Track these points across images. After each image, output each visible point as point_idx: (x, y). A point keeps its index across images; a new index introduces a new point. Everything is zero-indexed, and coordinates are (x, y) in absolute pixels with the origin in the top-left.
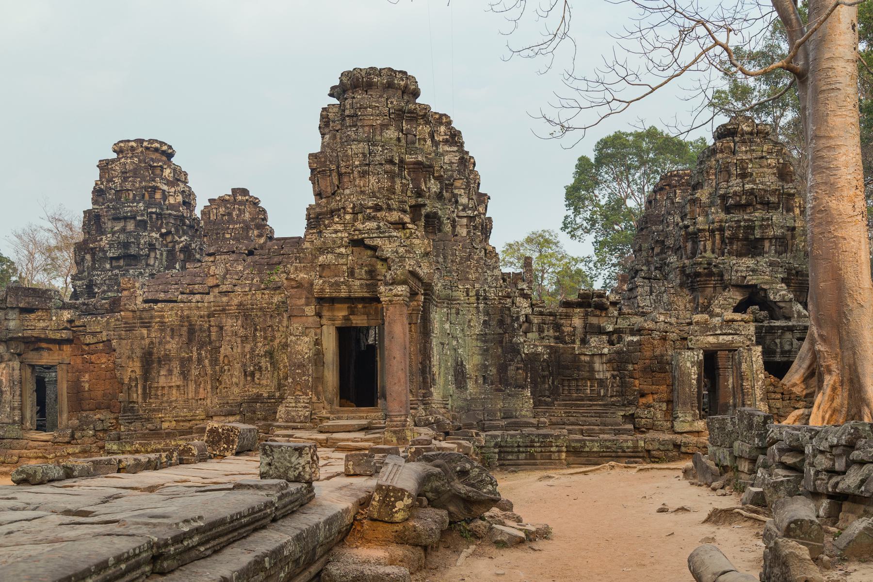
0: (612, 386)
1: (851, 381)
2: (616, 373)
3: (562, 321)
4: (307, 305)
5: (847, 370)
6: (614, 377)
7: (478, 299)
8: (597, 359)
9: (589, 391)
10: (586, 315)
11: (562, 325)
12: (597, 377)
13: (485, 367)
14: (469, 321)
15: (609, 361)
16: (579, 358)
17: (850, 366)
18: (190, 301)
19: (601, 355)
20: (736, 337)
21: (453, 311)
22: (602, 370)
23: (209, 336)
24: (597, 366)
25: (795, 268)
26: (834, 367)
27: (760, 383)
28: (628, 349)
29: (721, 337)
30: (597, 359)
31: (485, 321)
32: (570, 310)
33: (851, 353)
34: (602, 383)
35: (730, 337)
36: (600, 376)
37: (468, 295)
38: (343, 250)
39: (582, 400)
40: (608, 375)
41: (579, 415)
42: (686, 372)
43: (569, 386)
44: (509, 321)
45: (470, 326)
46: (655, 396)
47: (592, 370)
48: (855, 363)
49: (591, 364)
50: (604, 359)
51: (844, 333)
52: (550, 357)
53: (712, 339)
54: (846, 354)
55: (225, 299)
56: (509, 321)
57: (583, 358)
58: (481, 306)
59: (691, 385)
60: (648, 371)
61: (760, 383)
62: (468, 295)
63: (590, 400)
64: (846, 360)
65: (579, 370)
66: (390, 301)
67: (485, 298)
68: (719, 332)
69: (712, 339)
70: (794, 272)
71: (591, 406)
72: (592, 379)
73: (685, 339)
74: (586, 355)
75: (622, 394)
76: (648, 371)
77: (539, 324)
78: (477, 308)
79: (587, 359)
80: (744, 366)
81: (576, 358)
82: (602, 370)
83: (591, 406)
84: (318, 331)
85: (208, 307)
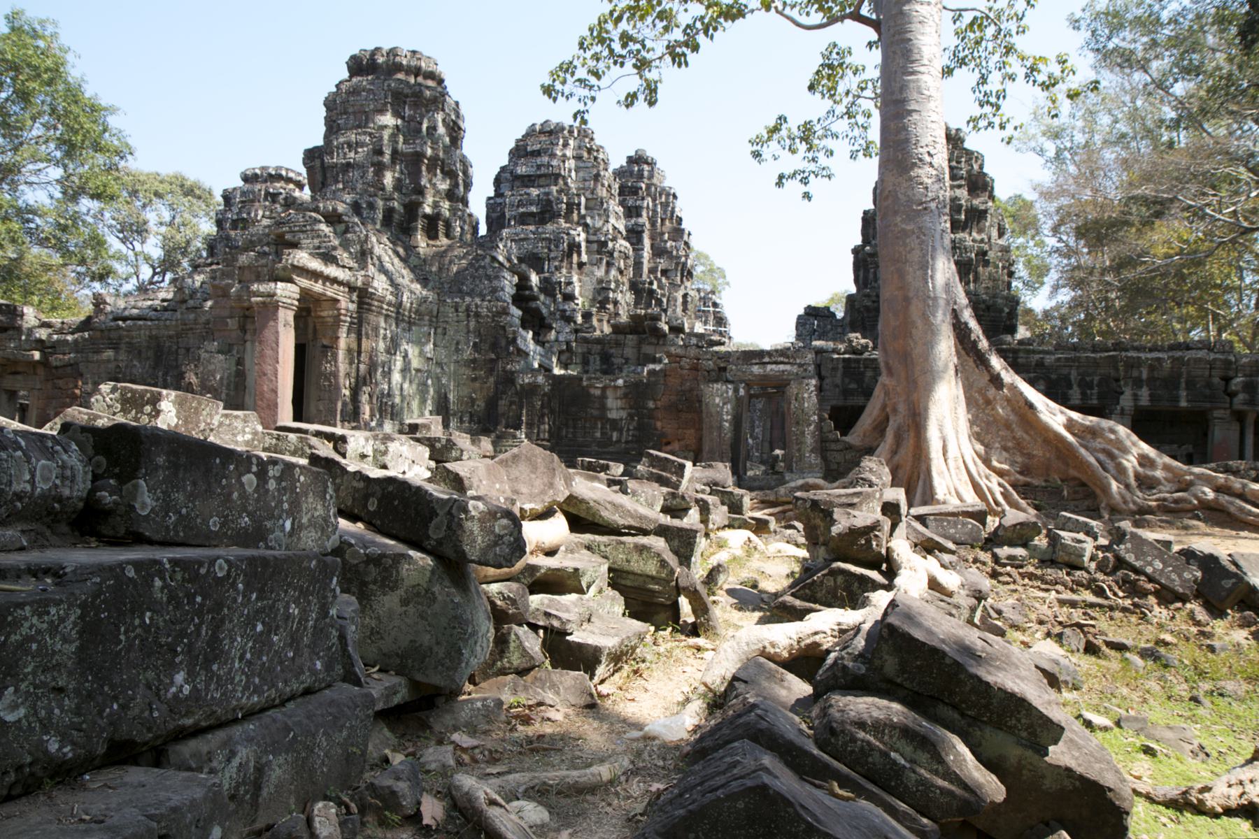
0: (628, 430)
3: (612, 351)
4: (231, 317)
6: (631, 416)
7: (468, 316)
9: (598, 435)
10: (640, 343)
11: (611, 355)
12: (610, 416)
13: (473, 401)
14: (458, 343)
15: (625, 396)
18: (158, 319)
19: (616, 387)
20: (788, 367)
21: (439, 331)
22: (616, 408)
23: (176, 360)
24: (612, 402)
25: (984, 301)
27: (812, 428)
30: (609, 393)
31: (475, 344)
32: (621, 337)
34: (615, 424)
35: (782, 367)
36: (613, 415)
37: (457, 311)
38: (266, 249)
40: (623, 414)
42: (713, 410)
43: (575, 427)
44: (503, 343)
45: (457, 350)
47: (603, 408)
49: (603, 397)
50: (619, 393)
52: (552, 390)
53: (756, 369)
55: (192, 316)
56: (503, 343)
57: (592, 391)
58: (472, 324)
59: (720, 427)
60: (673, 409)
61: (812, 428)
62: (457, 311)
66: (264, 303)
67: (477, 315)
68: (766, 359)
69: (756, 369)
70: (983, 306)
72: (603, 417)
73: (724, 369)
76: (673, 409)
77: (583, 354)
78: (467, 325)
79: (598, 392)
81: (585, 393)
82: (616, 408)
84: (241, 348)
85: (177, 326)
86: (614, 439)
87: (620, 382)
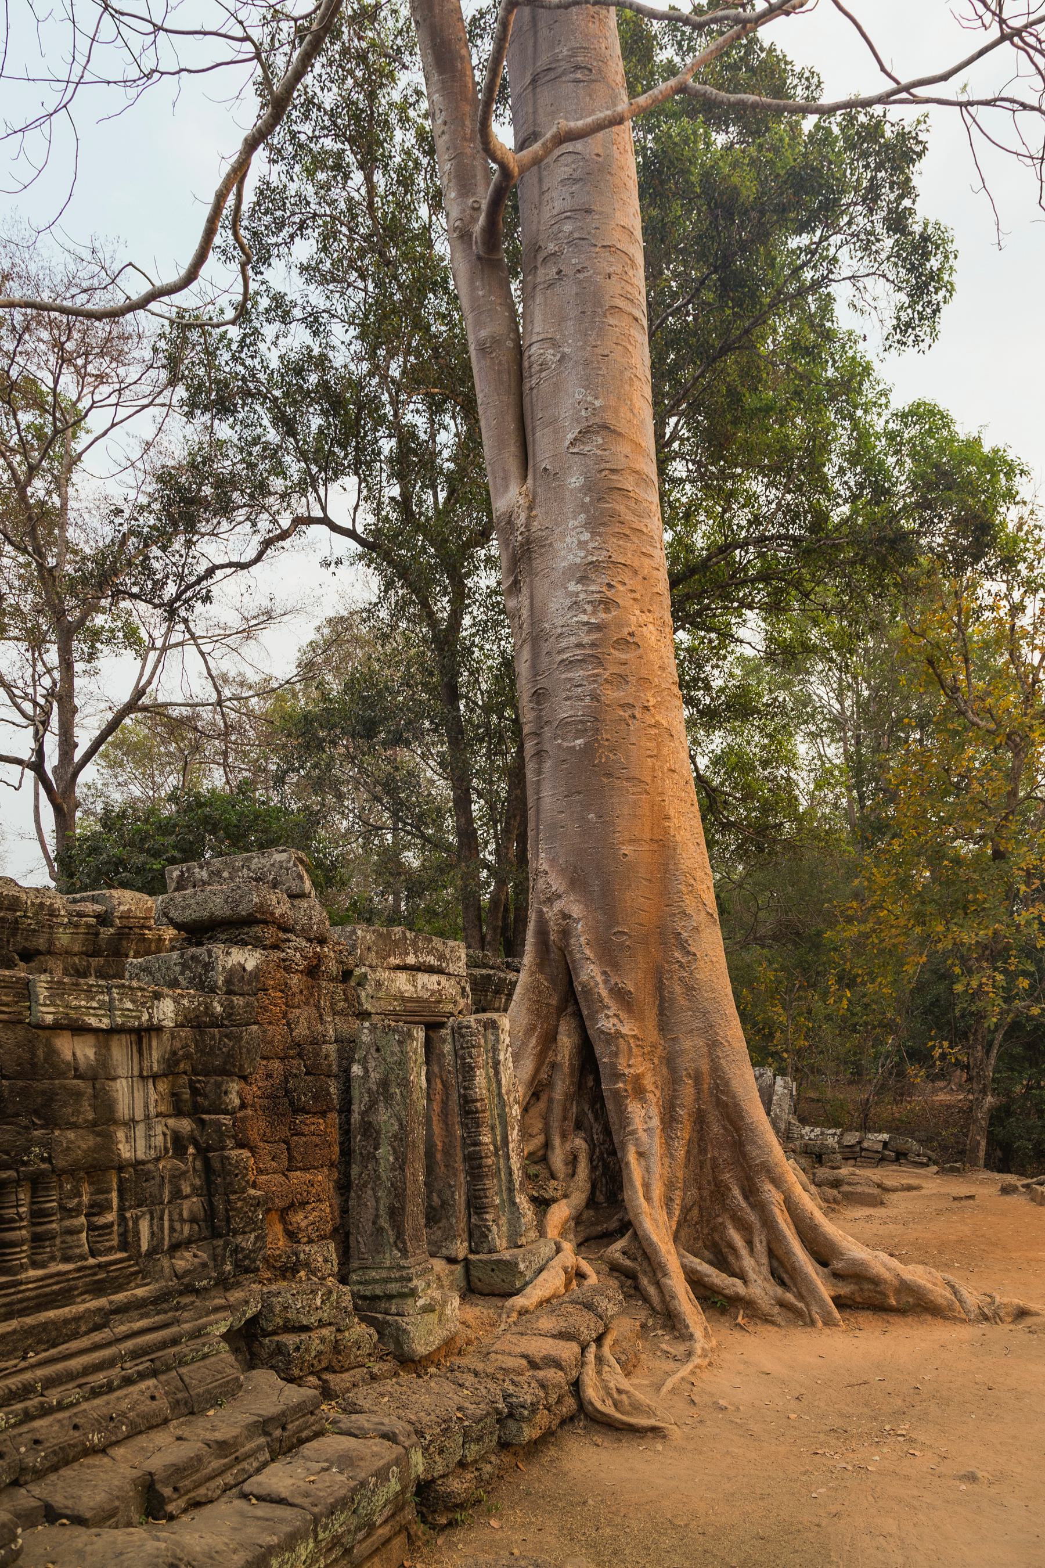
1: (700, 1119)
2: (185, 1125)
5: (687, 1090)
8: (120, 1053)
12: (125, 1151)
16: (52, 1052)
17: (697, 1078)
19: (141, 1035)
26: (648, 1082)
28: (230, 1010)
29: (423, 978)
33: (700, 1042)
39: (64, 1297)
41: (71, 1392)
46: (298, 1218)
47: (106, 1118)
48: (716, 1069)
49: (99, 1075)
50: (156, 1053)
51: (678, 989)
54: (686, 1044)
63: (98, 1289)
64: (685, 1064)
65: (51, 1122)
71: (103, 1319)
74: (79, 1029)
75: (214, 1225)
80: (481, 1079)
83: (103, 1319)
86: (144, 1246)
87: (166, 1011)
